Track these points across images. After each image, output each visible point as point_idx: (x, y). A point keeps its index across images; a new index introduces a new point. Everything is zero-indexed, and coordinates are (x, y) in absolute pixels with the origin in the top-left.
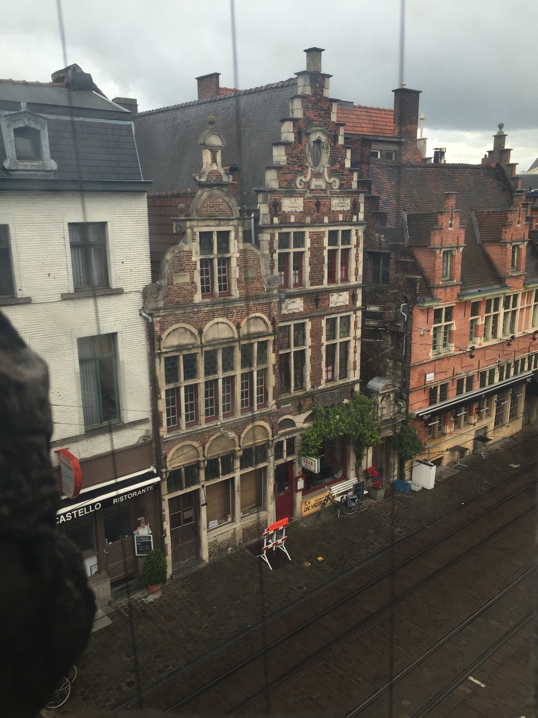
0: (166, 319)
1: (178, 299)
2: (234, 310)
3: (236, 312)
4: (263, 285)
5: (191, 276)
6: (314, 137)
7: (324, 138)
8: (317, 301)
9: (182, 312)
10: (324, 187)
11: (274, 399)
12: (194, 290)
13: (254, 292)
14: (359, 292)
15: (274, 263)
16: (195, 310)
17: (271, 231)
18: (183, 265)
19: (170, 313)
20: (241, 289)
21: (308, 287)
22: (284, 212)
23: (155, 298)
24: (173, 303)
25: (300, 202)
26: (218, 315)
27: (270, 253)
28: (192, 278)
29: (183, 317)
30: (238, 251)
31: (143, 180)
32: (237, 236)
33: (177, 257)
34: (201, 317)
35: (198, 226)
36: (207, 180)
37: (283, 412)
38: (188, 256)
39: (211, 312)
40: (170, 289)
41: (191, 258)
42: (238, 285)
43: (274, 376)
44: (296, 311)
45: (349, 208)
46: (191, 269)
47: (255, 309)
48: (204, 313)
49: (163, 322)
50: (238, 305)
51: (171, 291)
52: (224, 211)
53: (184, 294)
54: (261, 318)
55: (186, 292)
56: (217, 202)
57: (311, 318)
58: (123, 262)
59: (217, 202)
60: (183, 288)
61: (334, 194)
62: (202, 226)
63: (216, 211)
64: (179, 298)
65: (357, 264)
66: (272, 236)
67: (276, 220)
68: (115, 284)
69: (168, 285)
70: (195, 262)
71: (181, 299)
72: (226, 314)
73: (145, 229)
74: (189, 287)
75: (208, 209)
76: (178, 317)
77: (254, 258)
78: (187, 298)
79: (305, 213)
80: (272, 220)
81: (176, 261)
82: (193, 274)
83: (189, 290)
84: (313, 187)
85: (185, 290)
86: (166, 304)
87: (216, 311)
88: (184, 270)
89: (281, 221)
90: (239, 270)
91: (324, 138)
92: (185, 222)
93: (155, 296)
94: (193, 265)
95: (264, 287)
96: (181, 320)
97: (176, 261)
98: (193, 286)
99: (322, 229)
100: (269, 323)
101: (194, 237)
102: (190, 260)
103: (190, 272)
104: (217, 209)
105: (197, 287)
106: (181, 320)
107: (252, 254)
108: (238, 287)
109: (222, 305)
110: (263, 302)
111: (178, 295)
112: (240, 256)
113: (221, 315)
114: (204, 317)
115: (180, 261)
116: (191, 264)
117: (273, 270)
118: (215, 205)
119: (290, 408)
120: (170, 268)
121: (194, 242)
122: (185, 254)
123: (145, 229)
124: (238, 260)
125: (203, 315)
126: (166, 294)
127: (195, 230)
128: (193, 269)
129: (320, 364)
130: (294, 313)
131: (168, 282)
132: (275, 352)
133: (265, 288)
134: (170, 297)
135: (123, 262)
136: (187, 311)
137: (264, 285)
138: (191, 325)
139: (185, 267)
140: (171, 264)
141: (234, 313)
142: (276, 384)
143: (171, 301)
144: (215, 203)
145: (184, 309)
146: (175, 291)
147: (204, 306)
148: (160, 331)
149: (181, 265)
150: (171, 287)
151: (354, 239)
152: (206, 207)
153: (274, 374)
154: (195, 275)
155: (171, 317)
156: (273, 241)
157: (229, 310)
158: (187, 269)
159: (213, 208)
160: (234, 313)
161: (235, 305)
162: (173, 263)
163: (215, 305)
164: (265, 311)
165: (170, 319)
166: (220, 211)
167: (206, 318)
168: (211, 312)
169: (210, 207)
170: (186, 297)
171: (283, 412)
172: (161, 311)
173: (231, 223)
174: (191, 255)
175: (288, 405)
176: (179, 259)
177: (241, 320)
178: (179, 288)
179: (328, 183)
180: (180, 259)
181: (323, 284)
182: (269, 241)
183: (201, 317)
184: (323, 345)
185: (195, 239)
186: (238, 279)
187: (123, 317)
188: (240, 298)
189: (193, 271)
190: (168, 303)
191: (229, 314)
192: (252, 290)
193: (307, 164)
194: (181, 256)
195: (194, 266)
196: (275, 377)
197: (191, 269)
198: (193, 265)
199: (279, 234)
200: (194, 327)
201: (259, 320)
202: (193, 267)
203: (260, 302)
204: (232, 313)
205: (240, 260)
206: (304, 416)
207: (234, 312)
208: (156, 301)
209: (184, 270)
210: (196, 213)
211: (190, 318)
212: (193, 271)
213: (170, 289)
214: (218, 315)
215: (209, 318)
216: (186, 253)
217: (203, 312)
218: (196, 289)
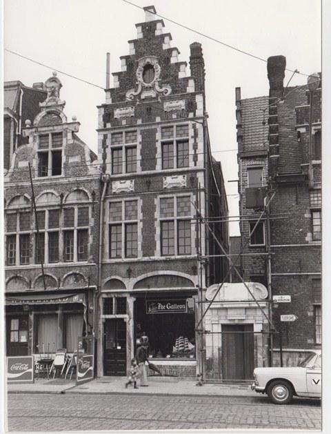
6: (141, 64)
7: (155, 62)
8: (149, 183)
10: (154, 95)
14: (200, 176)
17: (105, 133)
21: (139, 171)
25: (130, 111)
44: (126, 190)
45: (184, 108)
54: (85, 192)
57: (143, 197)
61: (164, 99)
65: (195, 151)
67: (109, 126)
79: (136, 117)
84: (143, 97)
91: (155, 62)
99: (153, 127)
100: (89, 194)
129: (154, 237)
130: (123, 192)
150: (16, 170)
151: (191, 132)
179: (159, 92)
181: (155, 169)
184: (156, 219)
193: (137, 83)
206: (134, 281)
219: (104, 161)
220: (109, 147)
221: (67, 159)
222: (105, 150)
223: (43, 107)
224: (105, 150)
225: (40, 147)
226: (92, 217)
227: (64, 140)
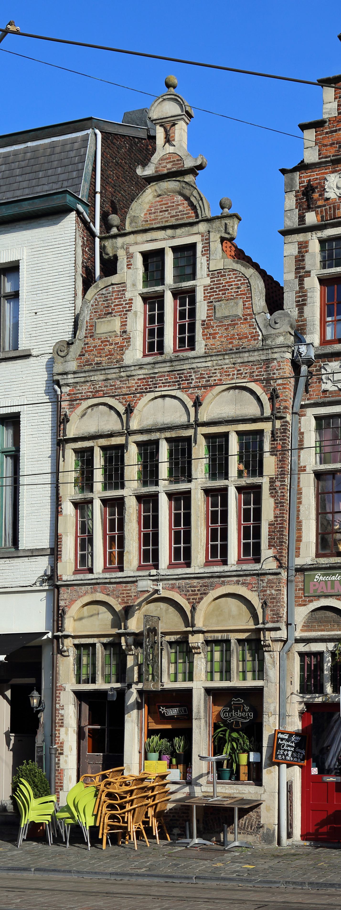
0: (79, 390)
1: (99, 359)
2: (193, 374)
3: (197, 378)
4: (255, 328)
5: (122, 322)
9: (102, 377)
11: (270, 546)
12: (125, 344)
13: (235, 342)
15: (306, 296)
16: (122, 374)
17: (300, 237)
18: (111, 306)
19: (82, 380)
20: (209, 338)
22: (328, 199)
23: (62, 357)
24: (91, 364)
26: (163, 383)
27: (296, 277)
28: (124, 324)
29: (105, 387)
30: (208, 275)
31: (80, 197)
32: (209, 250)
33: (103, 294)
34: (133, 386)
35: (136, 243)
36: (156, 172)
37: (319, 591)
38: (119, 291)
39: (151, 378)
40: (87, 344)
41: (124, 294)
42: (203, 332)
43: (272, 501)
46: (123, 311)
47: (236, 372)
48: (139, 379)
49: (74, 394)
50: (199, 365)
51: (90, 347)
52: (186, 214)
53: (109, 351)
55: (112, 347)
56: (173, 202)
58: (36, 313)
59: (173, 202)
60: (108, 341)
62: (143, 243)
63: (171, 217)
64: (100, 357)
66: (303, 247)
68: (23, 345)
69: (85, 337)
70: (129, 300)
71: (104, 359)
72: (178, 381)
73: (70, 262)
74: (119, 340)
75: (157, 216)
76: (97, 386)
77: (239, 283)
78: (113, 357)
80: (302, 218)
81: (101, 301)
82: (126, 318)
83: (118, 343)
85: (112, 344)
86: (81, 366)
87: (160, 377)
88: (111, 313)
89: (322, 217)
90: (208, 306)
92: (114, 240)
93: (62, 354)
94: (126, 304)
95: (256, 332)
96: (101, 391)
97: (101, 301)
98: (125, 337)
100: (265, 398)
101: (130, 261)
102: (122, 298)
103: (120, 315)
104: (173, 213)
105: (130, 338)
106: (101, 391)
107: (236, 277)
108: (203, 335)
109: (168, 364)
110: (251, 359)
111: (100, 353)
112: (211, 282)
113: (170, 382)
114: (138, 386)
115: (107, 300)
116: (124, 303)
117: (303, 309)
118: (169, 207)
119: (337, 584)
120: (92, 313)
121: (130, 268)
122: (116, 289)
123: (70, 262)
124: (207, 290)
125: (136, 383)
126: (82, 352)
127: (132, 250)
128: (126, 311)
131: (86, 334)
132: (276, 455)
133: (260, 333)
134: (87, 355)
135: (36, 313)
136: (109, 377)
137: (258, 330)
138: (116, 399)
139: (113, 309)
140: (92, 305)
141: (192, 379)
142: (276, 517)
143: (88, 363)
144: (169, 205)
145: (103, 372)
146: (95, 346)
147: (137, 367)
148: (69, 409)
149: (107, 307)
150: (90, 340)
152: (155, 213)
153: (272, 497)
154: (128, 319)
155: (87, 387)
156: (303, 256)
157: (183, 374)
158: (116, 312)
159: (167, 213)
160: (192, 379)
161: (194, 366)
162: (96, 305)
163: (157, 366)
164: (257, 376)
165: (85, 389)
166: (178, 215)
167: (142, 389)
168: (151, 378)
169: (161, 212)
170: (112, 355)
171: (319, 591)
172: (70, 376)
173: (195, 229)
174: (123, 290)
175: (333, 578)
176: (105, 297)
177: (205, 392)
178: (102, 342)
180: (107, 297)
182: (296, 258)
183: (133, 386)
185: (131, 265)
186: (204, 321)
187: (31, 390)
188: (205, 353)
189: (126, 314)
190: (84, 366)
191: (182, 380)
192: (231, 339)
194: (109, 293)
195: (127, 306)
196: (276, 503)
197: (123, 311)
198: (126, 304)
199: (322, 242)
200: (120, 402)
201: (248, 394)
202: (126, 307)
203: (246, 360)
204: (189, 380)
205: (211, 289)
207: (193, 377)
208: (66, 362)
209: (111, 313)
210: (130, 224)
211: (116, 389)
212: (126, 314)
213: (87, 344)
214: (163, 383)
215: (146, 389)
216: (117, 288)
217: (136, 378)
218: (129, 341)
219: (301, 312)
220: (314, 274)
221: (212, 308)
222: (301, 283)
223: (150, 180)
224: (301, 283)
225: (148, 281)
226: (273, 452)
227: (201, 261)
